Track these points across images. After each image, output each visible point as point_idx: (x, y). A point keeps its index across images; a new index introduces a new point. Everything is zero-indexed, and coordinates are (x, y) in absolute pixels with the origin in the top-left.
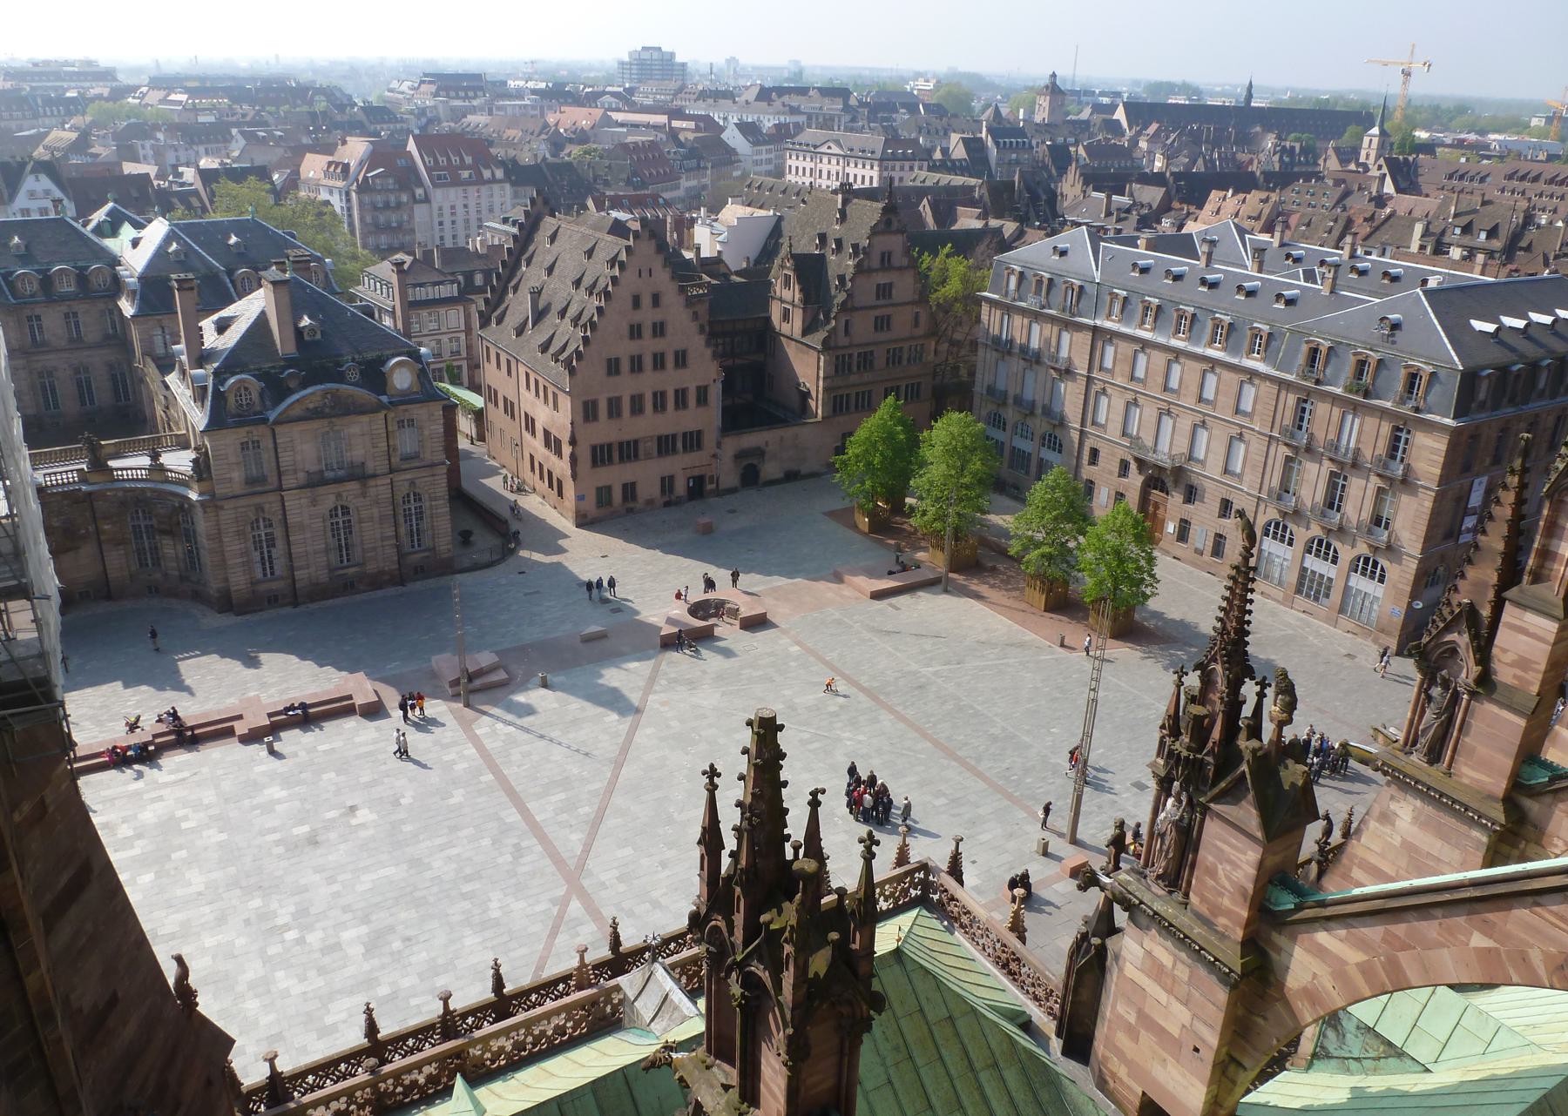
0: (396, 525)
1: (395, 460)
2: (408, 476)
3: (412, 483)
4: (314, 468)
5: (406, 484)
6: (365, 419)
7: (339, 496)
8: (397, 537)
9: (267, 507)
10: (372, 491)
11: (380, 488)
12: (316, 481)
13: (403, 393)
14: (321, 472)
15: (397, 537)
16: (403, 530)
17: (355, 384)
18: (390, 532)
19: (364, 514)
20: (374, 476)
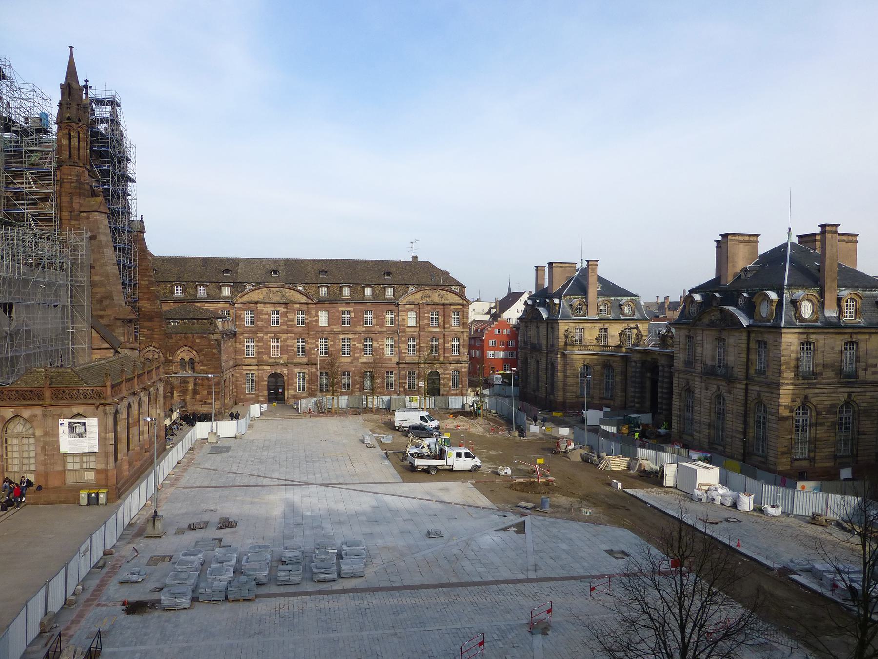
0: (746, 423)
1: (752, 372)
2: (757, 388)
3: (759, 396)
4: (710, 363)
5: (755, 393)
6: (737, 334)
7: (718, 387)
8: (745, 433)
9: (691, 382)
10: (735, 391)
11: (739, 390)
12: (710, 373)
13: (763, 319)
14: (713, 366)
15: (745, 433)
16: (751, 432)
17: (740, 309)
18: (740, 428)
19: (729, 406)
20: (736, 379)
